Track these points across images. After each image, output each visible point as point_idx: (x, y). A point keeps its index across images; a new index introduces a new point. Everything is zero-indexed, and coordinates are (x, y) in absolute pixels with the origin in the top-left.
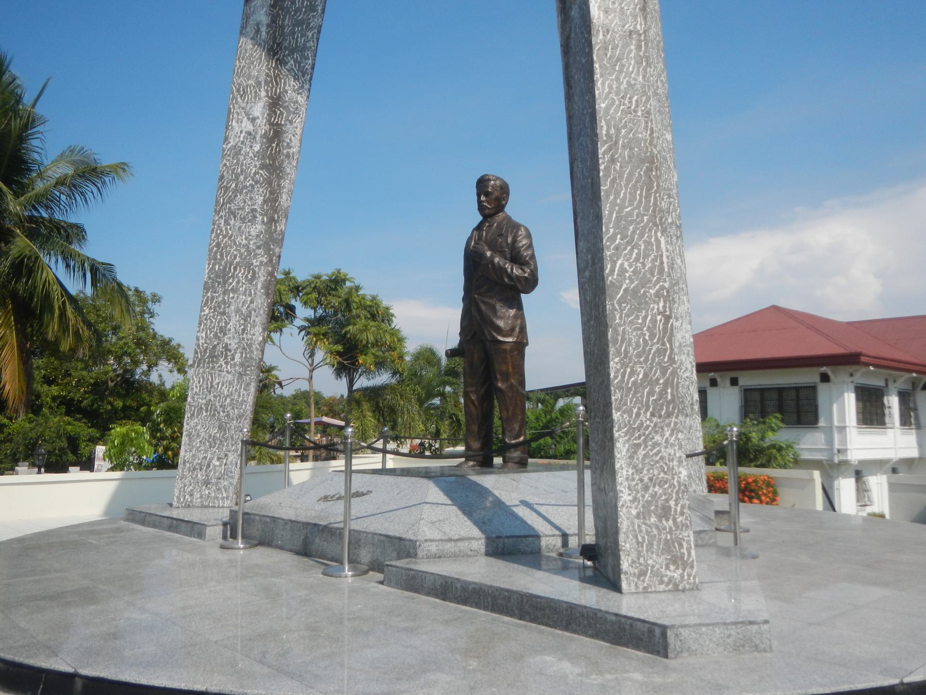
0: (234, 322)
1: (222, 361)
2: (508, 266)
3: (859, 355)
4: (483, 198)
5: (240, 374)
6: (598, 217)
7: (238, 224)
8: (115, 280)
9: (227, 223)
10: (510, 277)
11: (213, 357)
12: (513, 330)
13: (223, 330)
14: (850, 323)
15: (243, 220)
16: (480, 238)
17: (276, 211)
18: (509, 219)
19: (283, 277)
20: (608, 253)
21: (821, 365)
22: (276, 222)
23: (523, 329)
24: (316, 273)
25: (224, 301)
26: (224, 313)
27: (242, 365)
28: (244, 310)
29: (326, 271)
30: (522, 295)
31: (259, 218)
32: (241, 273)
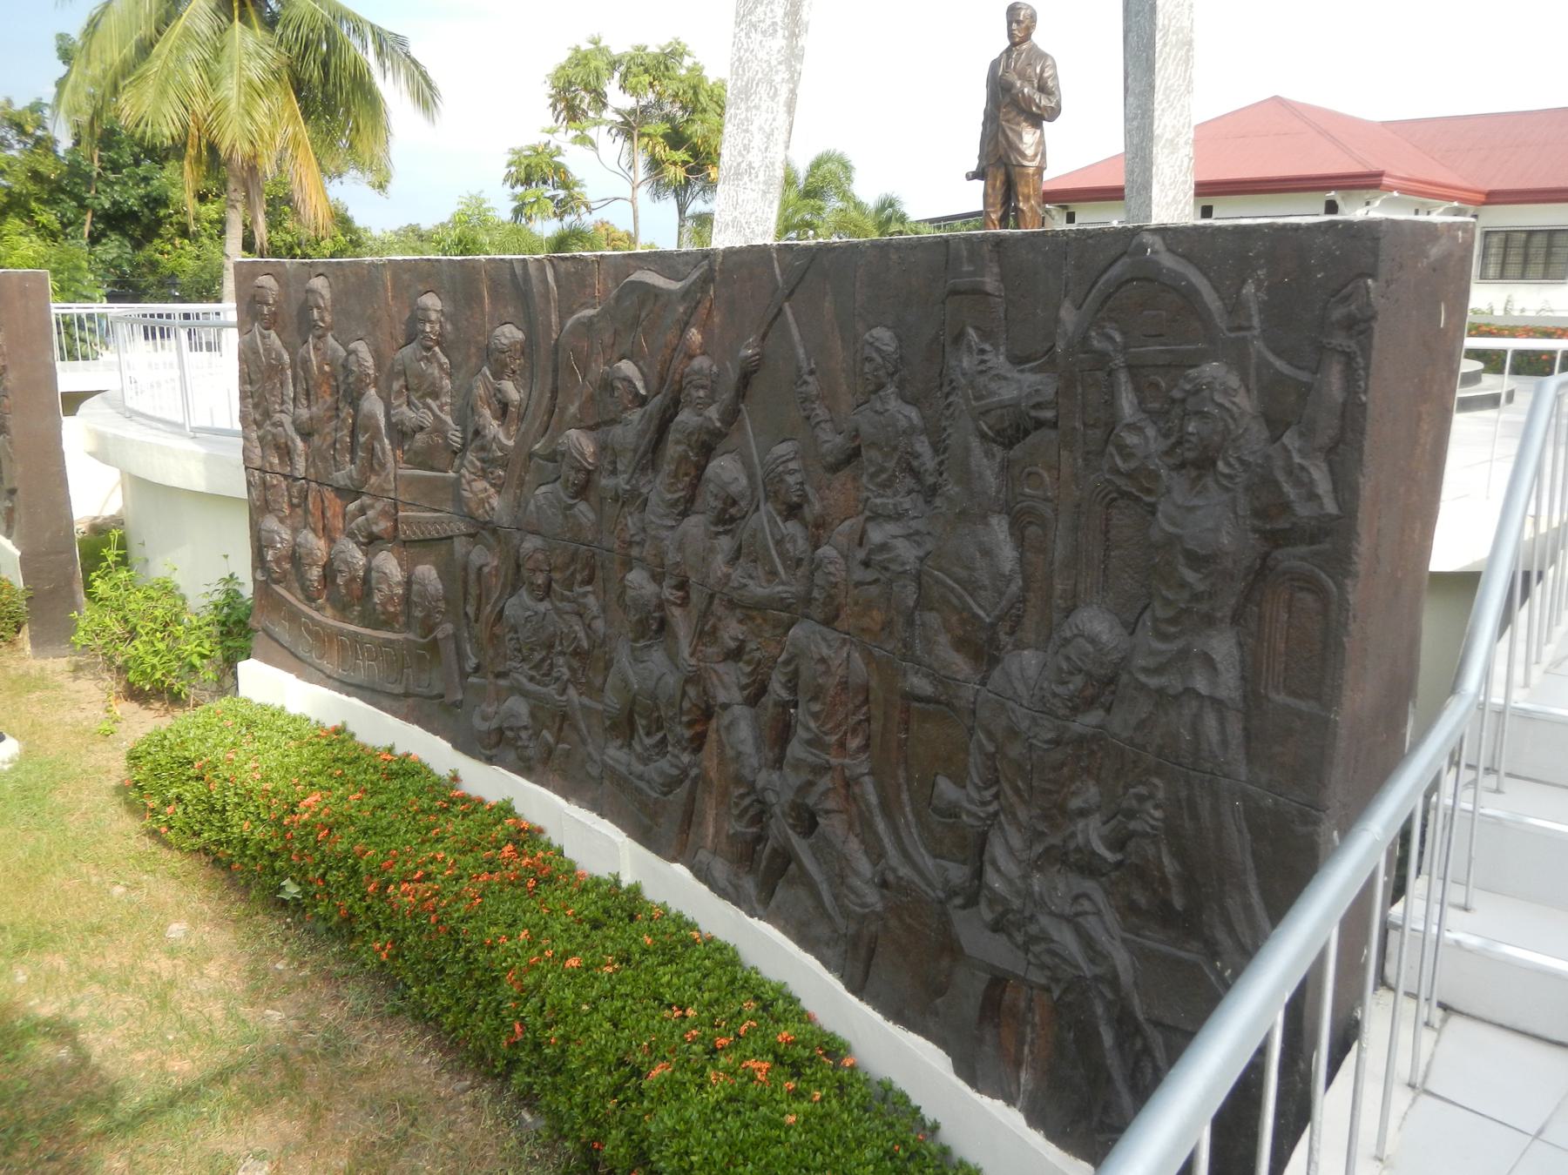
0: (758, 140)
1: (746, 178)
2: (1036, 97)
3: (1380, 175)
4: (1014, 26)
5: (764, 193)
6: (1152, 87)
7: (759, 37)
8: (407, 55)
9: (748, 36)
10: (1038, 107)
11: (738, 175)
12: (1036, 155)
13: (747, 148)
14: (1383, 123)
15: (764, 33)
16: (1007, 66)
17: (796, 25)
18: (1035, 46)
19: (592, 46)
20: (1157, 114)
21: (1329, 189)
22: (798, 36)
23: (1044, 155)
24: (640, 41)
25: (747, 119)
26: (747, 131)
27: (765, 183)
28: (767, 130)
29: (655, 43)
30: (1045, 123)
31: (780, 32)
32: (763, 89)
